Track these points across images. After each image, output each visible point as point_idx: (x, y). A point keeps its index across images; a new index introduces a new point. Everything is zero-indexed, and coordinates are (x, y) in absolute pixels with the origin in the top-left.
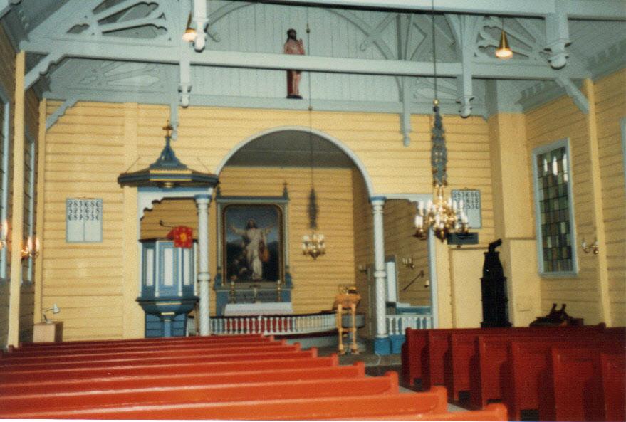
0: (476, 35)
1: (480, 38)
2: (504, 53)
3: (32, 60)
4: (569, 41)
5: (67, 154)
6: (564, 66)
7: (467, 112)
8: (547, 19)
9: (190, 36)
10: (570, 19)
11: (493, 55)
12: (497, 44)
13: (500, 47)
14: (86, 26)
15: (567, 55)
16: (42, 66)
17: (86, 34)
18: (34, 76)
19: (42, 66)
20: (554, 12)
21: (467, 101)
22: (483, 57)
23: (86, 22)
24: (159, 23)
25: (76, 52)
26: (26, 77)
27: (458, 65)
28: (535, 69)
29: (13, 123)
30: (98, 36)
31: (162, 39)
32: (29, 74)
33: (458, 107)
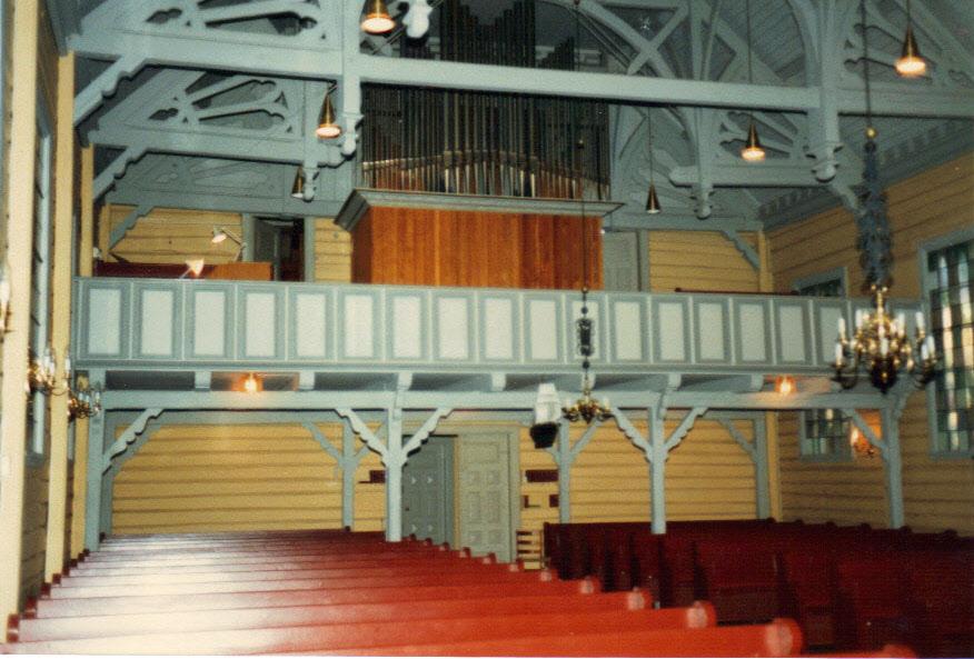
0: (718, 125)
1: (724, 128)
2: (753, 154)
3: (89, 67)
4: (839, 145)
5: (199, 453)
6: (833, 178)
7: (706, 211)
8: (809, 113)
9: (329, 130)
10: (841, 115)
11: (739, 155)
12: (744, 136)
13: (748, 145)
14: (173, 112)
15: (836, 163)
16: (118, 166)
17: (173, 122)
18: (107, 178)
19: (107, 81)
20: (818, 106)
21: (705, 196)
22: (727, 157)
23: (175, 105)
24: (277, 108)
25: (162, 146)
26: (98, 180)
27: (694, 169)
28: (792, 173)
29: (80, 161)
30: (194, 125)
31: (278, 130)
32: (101, 176)
33: (693, 203)
